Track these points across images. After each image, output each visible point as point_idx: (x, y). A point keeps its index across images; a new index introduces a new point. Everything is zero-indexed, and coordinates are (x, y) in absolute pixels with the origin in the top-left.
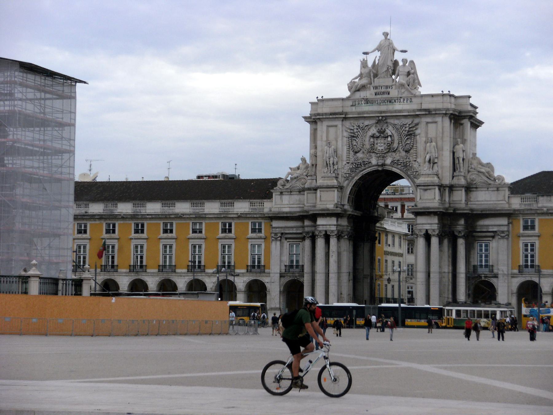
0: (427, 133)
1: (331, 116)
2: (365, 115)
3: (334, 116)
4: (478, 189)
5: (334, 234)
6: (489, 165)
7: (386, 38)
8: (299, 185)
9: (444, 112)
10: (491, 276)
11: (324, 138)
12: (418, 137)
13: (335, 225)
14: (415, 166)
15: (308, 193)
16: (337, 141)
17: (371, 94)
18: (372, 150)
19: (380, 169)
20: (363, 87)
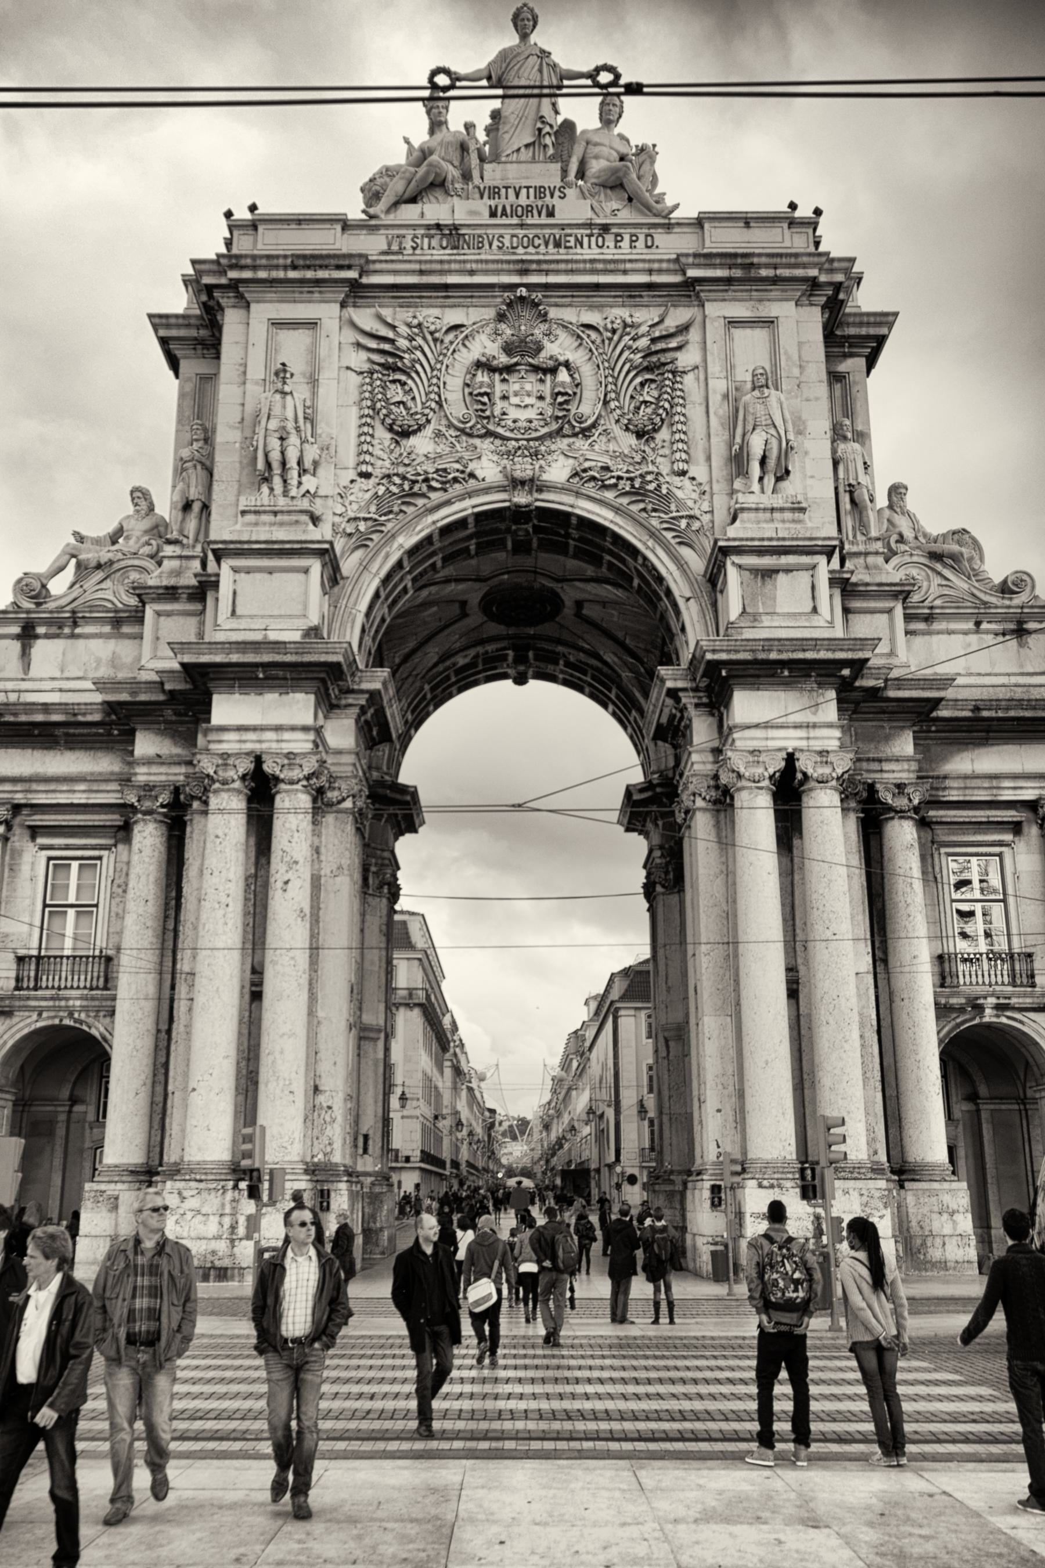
0: (730, 368)
1: (292, 274)
2: (452, 279)
3: (309, 274)
4: (936, 626)
5: (296, 774)
6: (960, 534)
7: (524, 37)
8: (115, 594)
9: (813, 272)
10: (1028, 1001)
11: (257, 371)
12: (689, 380)
13: (305, 729)
14: (679, 494)
15: (159, 614)
16: (313, 382)
17: (473, 213)
18: (482, 425)
19: (521, 498)
20: (437, 185)
